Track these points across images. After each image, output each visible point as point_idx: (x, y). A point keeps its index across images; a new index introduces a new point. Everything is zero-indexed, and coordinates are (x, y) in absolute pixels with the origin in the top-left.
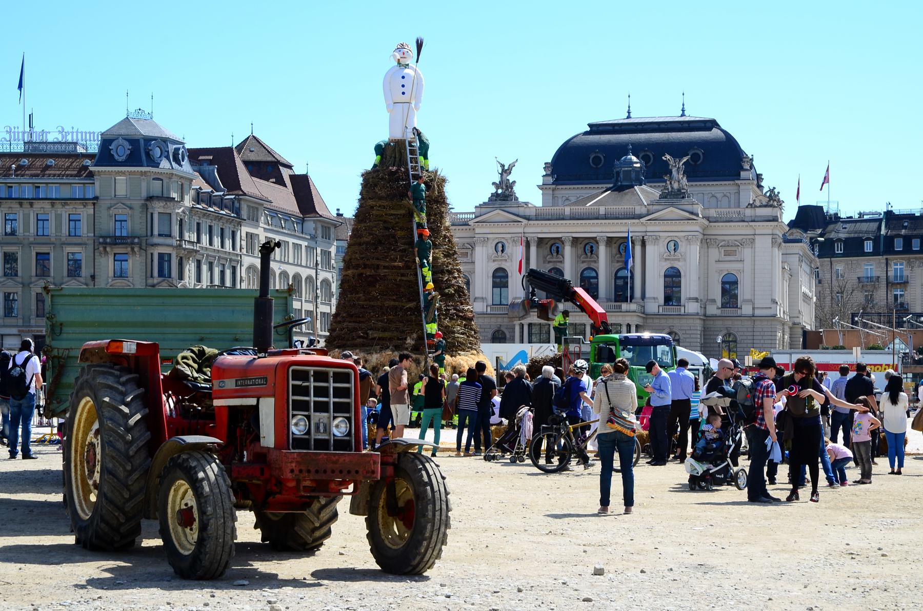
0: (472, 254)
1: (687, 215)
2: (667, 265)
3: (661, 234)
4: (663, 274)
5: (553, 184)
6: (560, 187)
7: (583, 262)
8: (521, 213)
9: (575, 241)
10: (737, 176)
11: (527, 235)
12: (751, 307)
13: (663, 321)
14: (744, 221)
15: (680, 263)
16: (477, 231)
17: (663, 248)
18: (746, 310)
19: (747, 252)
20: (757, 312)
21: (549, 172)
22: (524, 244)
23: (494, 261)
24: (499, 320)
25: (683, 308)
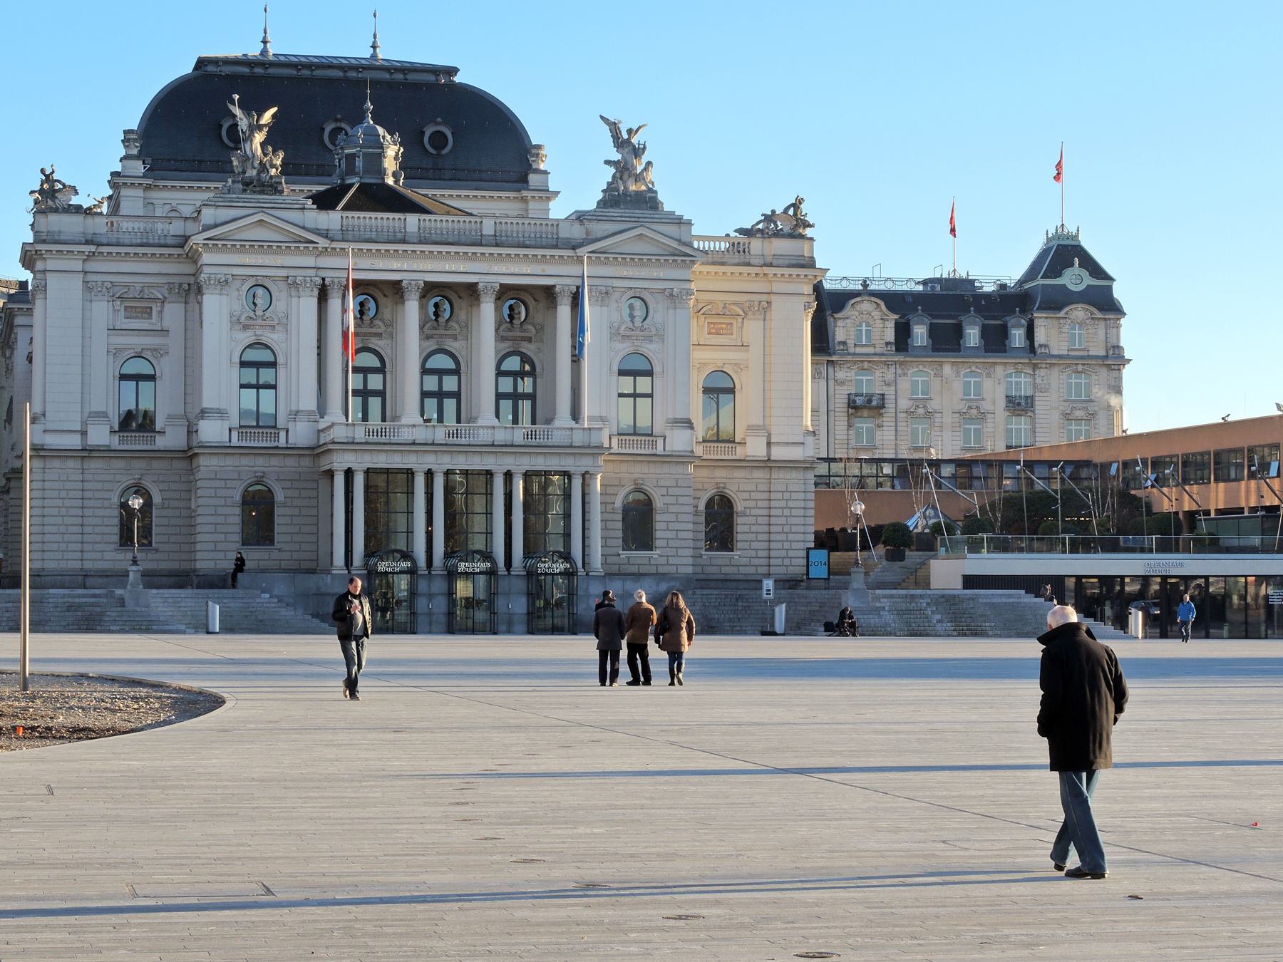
0: (161, 312)
1: (675, 244)
2: (625, 348)
3: (616, 283)
4: (615, 369)
5: (144, 176)
6: (162, 183)
7: (428, 337)
8: (309, 225)
9: (430, 289)
10: (526, 181)
11: (323, 274)
12: (764, 440)
13: (624, 467)
14: (749, 264)
15: (653, 347)
16: (206, 258)
17: (617, 312)
18: (755, 448)
19: (752, 329)
20: (778, 453)
21: (135, 151)
22: (316, 292)
23: (246, 327)
24: (260, 461)
25: (660, 442)
